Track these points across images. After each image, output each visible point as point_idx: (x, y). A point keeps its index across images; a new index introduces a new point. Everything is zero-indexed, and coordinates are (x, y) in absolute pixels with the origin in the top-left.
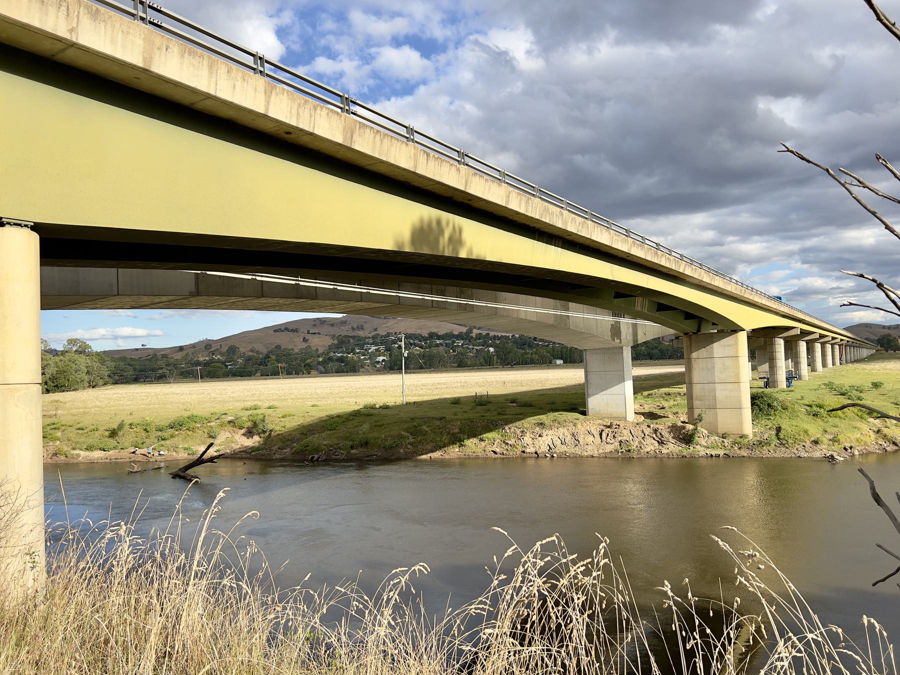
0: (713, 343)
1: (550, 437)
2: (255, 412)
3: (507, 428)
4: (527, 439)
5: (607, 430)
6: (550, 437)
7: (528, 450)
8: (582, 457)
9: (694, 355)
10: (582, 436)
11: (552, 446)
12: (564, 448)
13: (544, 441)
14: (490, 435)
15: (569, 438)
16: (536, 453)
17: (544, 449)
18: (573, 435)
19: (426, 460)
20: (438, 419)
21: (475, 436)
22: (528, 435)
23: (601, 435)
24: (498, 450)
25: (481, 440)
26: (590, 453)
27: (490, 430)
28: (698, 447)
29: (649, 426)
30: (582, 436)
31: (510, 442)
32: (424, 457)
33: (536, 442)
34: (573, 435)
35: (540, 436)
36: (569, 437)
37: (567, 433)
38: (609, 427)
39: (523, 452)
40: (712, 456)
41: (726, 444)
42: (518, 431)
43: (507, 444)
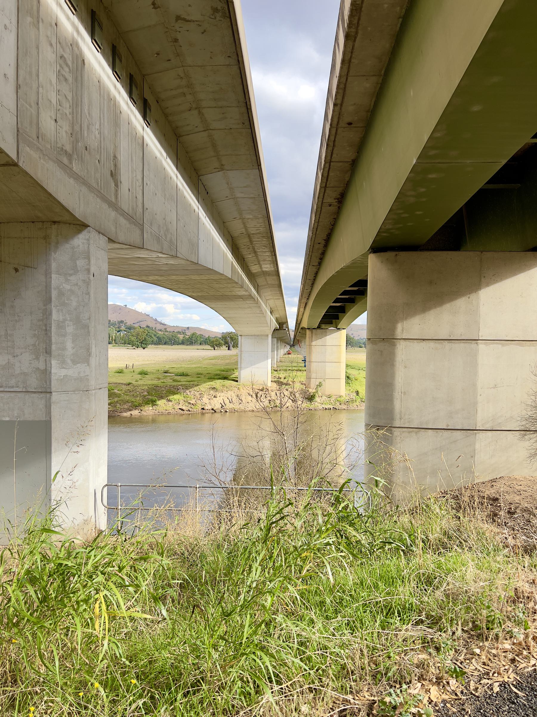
0: (326, 336)
1: (222, 398)
2: (115, 606)
3: (187, 391)
4: (205, 400)
5: (261, 393)
6: (222, 398)
7: (206, 408)
8: (245, 411)
9: (314, 343)
10: (244, 397)
11: (223, 404)
12: (231, 406)
13: (218, 401)
14: (176, 397)
15: (235, 399)
16: (212, 409)
17: (217, 407)
18: (238, 396)
19: (126, 417)
20: (125, 384)
21: (162, 398)
22: (205, 396)
23: (257, 396)
24: (184, 408)
25: (169, 401)
26: (250, 409)
27: (174, 394)
28: (316, 403)
29: (287, 390)
30: (244, 397)
31: (192, 402)
32: (125, 414)
33: (212, 401)
34: (238, 396)
35: (215, 397)
36: (235, 397)
37: (233, 395)
38: (262, 390)
39: (203, 409)
40: (326, 409)
42: (197, 394)
43: (190, 403)
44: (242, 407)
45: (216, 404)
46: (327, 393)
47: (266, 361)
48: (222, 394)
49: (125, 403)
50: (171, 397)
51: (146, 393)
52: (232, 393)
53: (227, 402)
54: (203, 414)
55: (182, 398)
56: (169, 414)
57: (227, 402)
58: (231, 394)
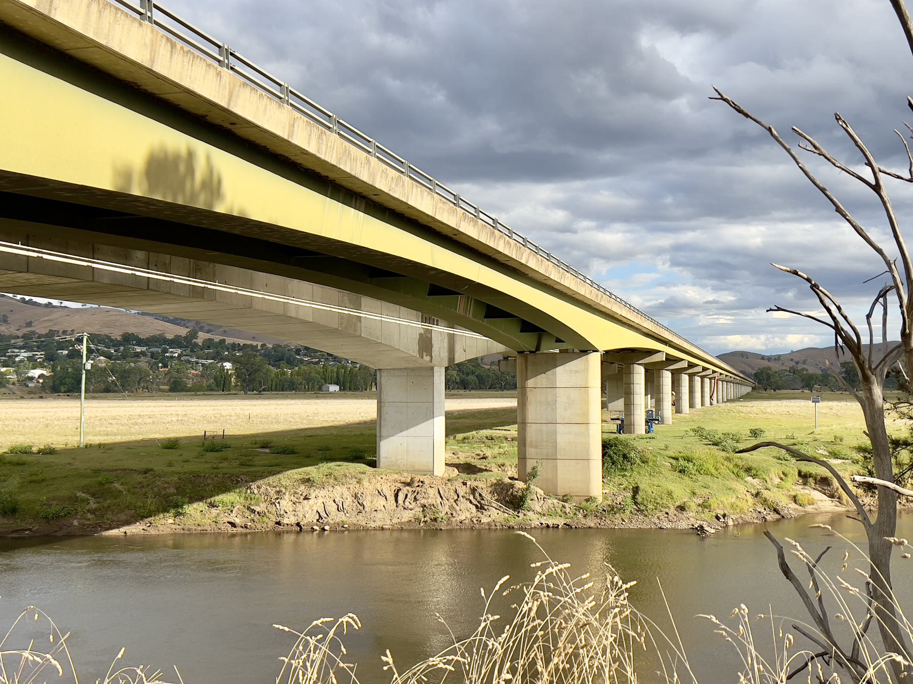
1: (320, 500)
4: (285, 504)
5: (405, 489)
6: (320, 500)
7: (286, 521)
8: (366, 530)
9: (531, 383)
10: (369, 498)
11: (323, 514)
12: (340, 517)
13: (311, 507)
14: (227, 497)
15: (349, 502)
16: (298, 524)
18: (356, 496)
22: (287, 496)
24: (238, 521)
25: (212, 505)
26: (379, 524)
27: (226, 489)
28: (530, 514)
29: (465, 484)
30: (369, 498)
31: (257, 509)
33: (299, 507)
34: (356, 496)
35: (306, 498)
36: (350, 499)
37: (346, 494)
38: (409, 484)
39: (278, 523)
40: (548, 526)
41: (568, 510)
42: (272, 492)
43: (253, 511)
44: (361, 520)
45: (308, 513)
46: (561, 492)
47: (431, 421)
48: (322, 493)
49: (122, 511)
50: (217, 498)
51: (172, 490)
52: (344, 489)
53: (332, 508)
54: (279, 534)
55: (242, 500)
56: (203, 533)
57: (332, 508)
58: (342, 493)
